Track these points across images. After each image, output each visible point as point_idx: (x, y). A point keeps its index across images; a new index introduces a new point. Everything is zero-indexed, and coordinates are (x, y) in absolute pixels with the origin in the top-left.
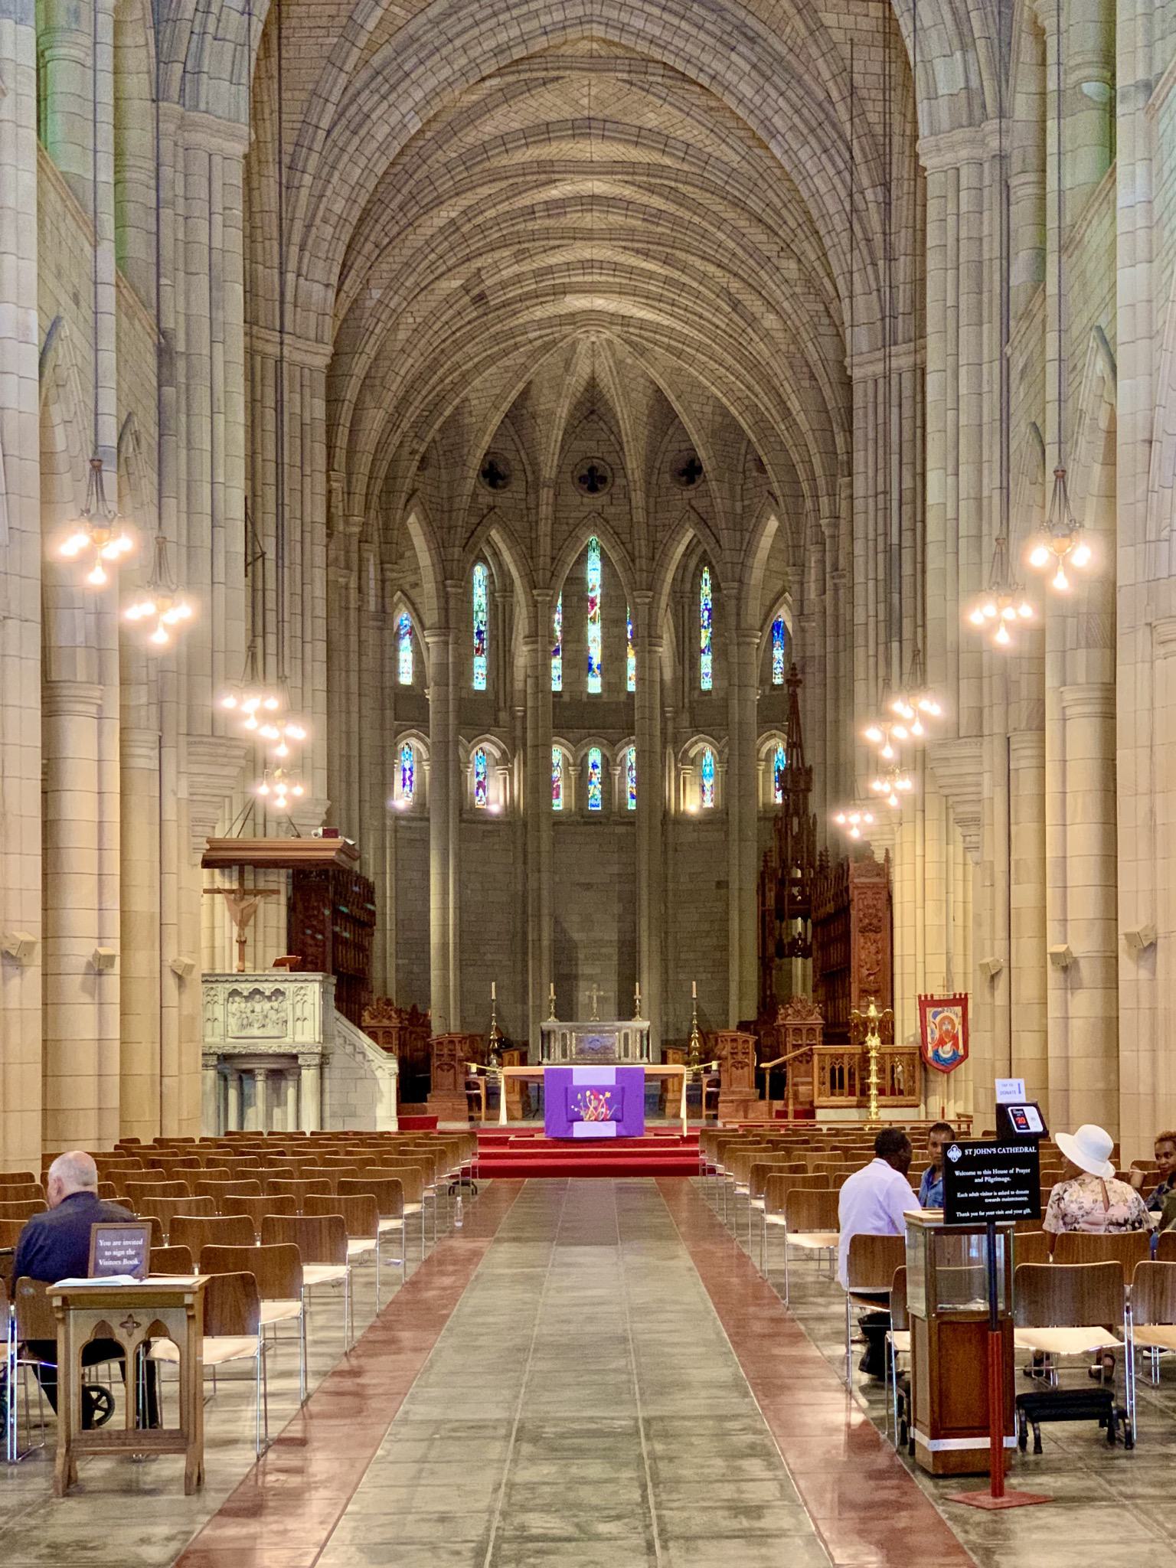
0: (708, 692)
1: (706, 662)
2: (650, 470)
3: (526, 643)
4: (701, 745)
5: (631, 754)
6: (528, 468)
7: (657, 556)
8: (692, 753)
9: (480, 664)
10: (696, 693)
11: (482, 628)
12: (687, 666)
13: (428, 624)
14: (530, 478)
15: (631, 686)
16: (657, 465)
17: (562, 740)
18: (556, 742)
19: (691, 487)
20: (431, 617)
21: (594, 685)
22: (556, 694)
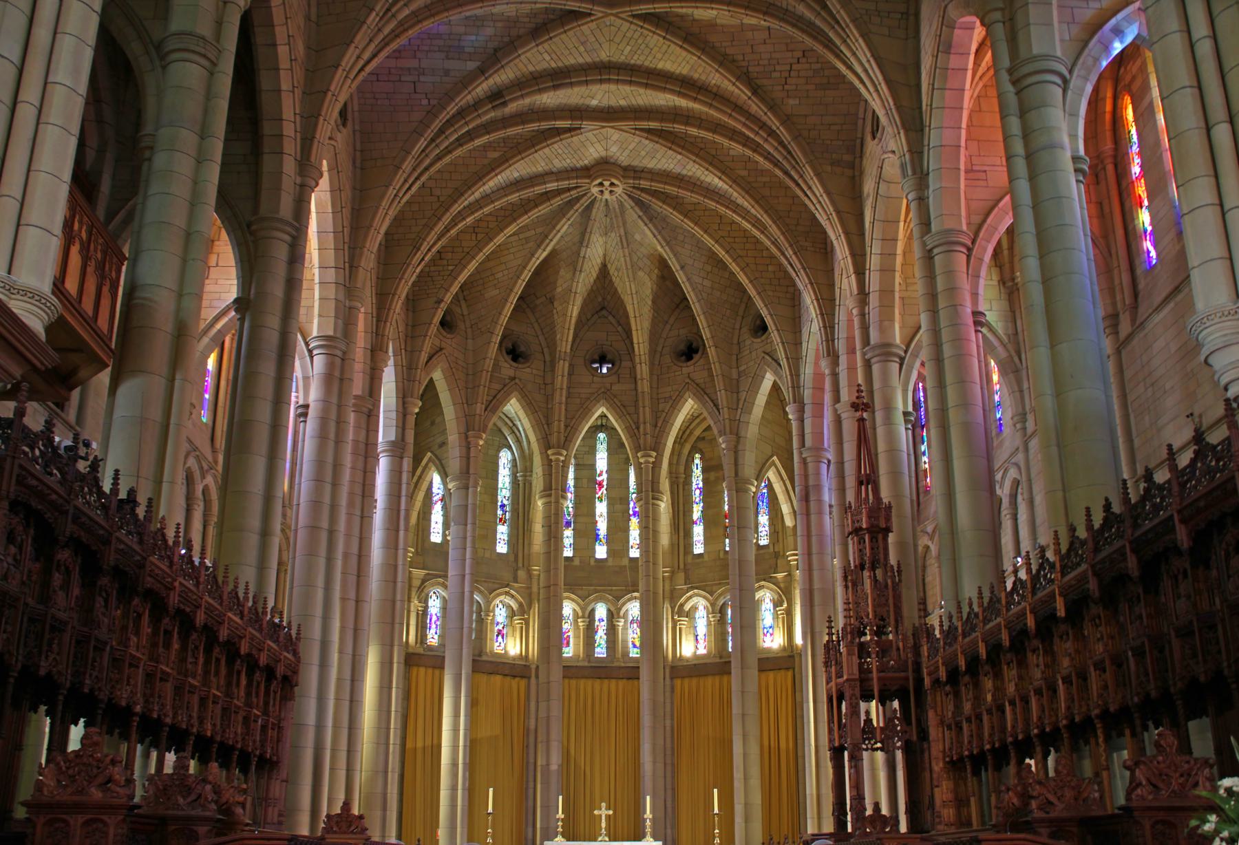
0: (700, 555)
1: (698, 531)
2: (653, 352)
3: (541, 497)
4: (695, 600)
5: (633, 609)
6: (546, 350)
7: (661, 423)
8: (687, 607)
9: (502, 531)
10: (689, 559)
11: (505, 502)
12: (682, 534)
13: (449, 470)
14: (548, 358)
15: (634, 553)
16: (659, 349)
17: (573, 596)
18: (568, 598)
19: (689, 363)
20: (454, 464)
21: (601, 552)
22: (567, 558)
